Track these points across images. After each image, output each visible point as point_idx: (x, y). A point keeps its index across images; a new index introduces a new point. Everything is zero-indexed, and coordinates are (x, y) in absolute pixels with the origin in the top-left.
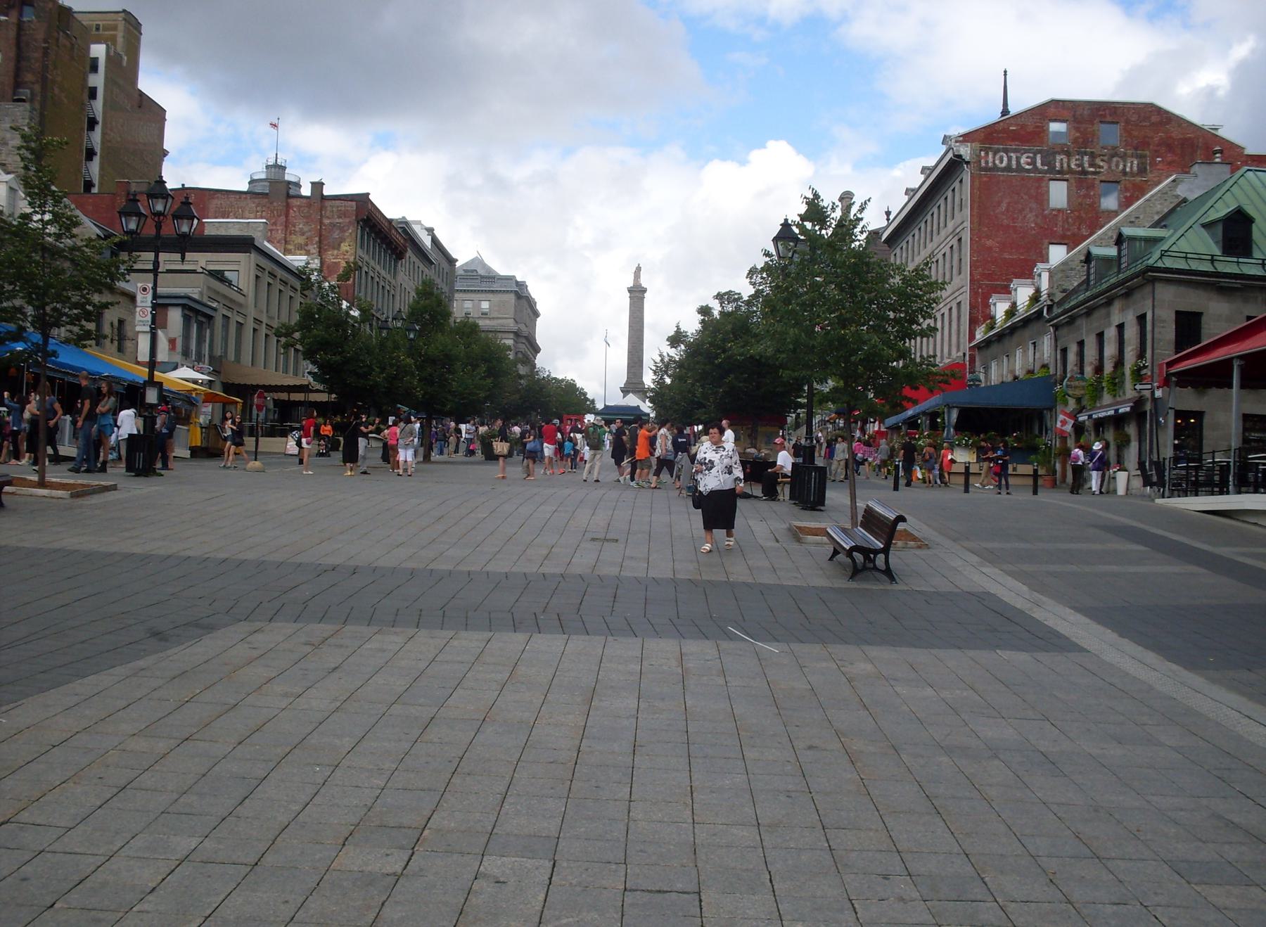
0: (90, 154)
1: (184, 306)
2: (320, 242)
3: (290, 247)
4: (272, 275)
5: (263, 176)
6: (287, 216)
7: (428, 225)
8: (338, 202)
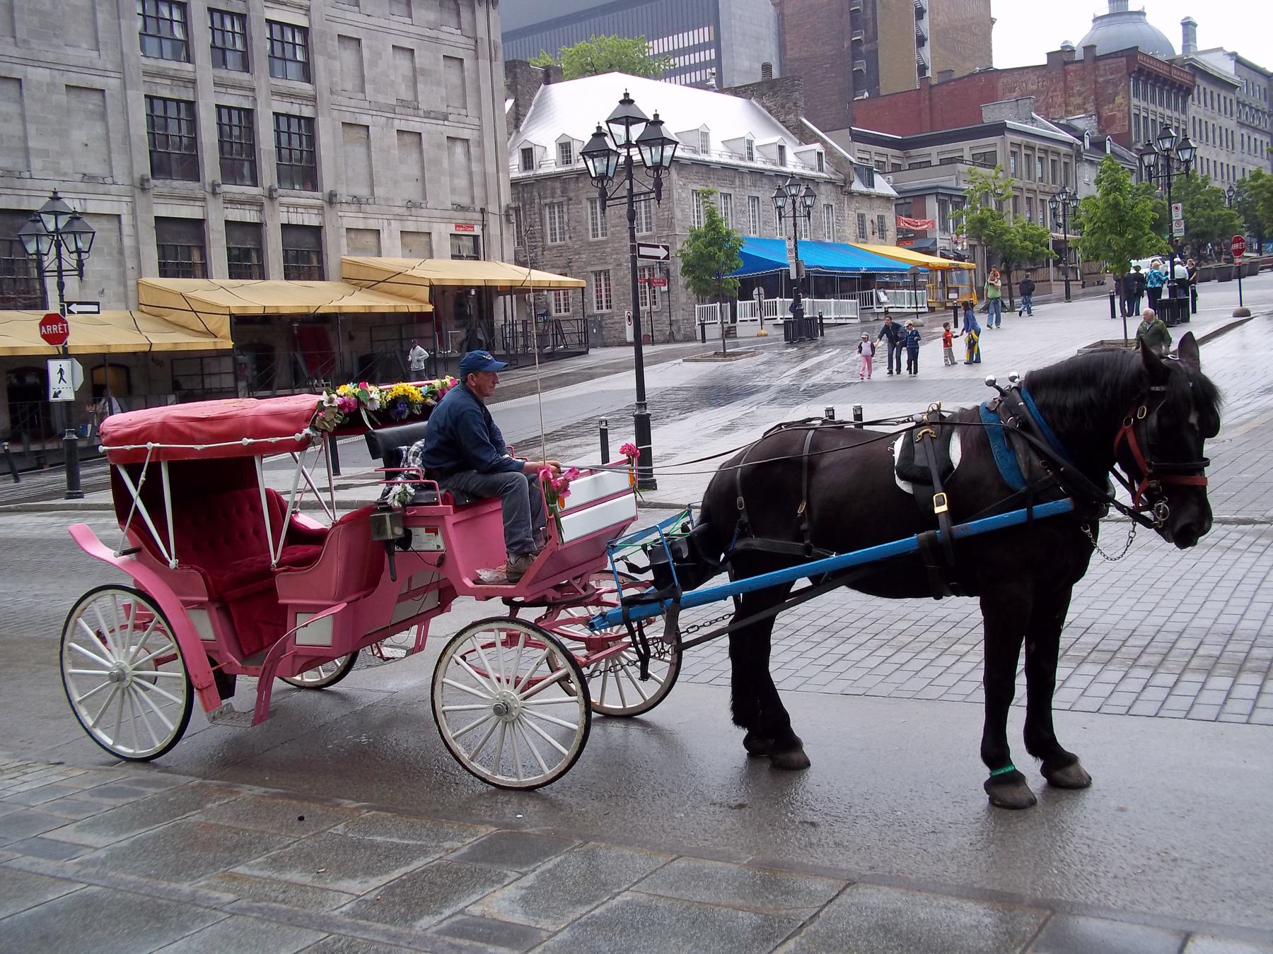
0: (921, 41)
1: (937, 194)
2: (1096, 99)
3: (1070, 108)
4: (1027, 147)
5: (1107, 12)
6: (1065, 81)
7: (1230, 50)
8: (1109, 61)
